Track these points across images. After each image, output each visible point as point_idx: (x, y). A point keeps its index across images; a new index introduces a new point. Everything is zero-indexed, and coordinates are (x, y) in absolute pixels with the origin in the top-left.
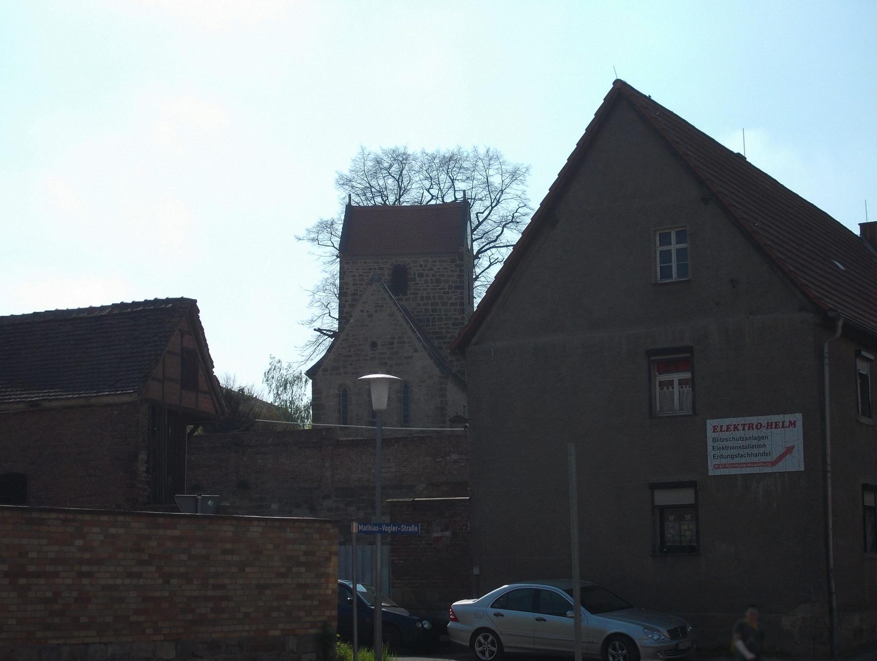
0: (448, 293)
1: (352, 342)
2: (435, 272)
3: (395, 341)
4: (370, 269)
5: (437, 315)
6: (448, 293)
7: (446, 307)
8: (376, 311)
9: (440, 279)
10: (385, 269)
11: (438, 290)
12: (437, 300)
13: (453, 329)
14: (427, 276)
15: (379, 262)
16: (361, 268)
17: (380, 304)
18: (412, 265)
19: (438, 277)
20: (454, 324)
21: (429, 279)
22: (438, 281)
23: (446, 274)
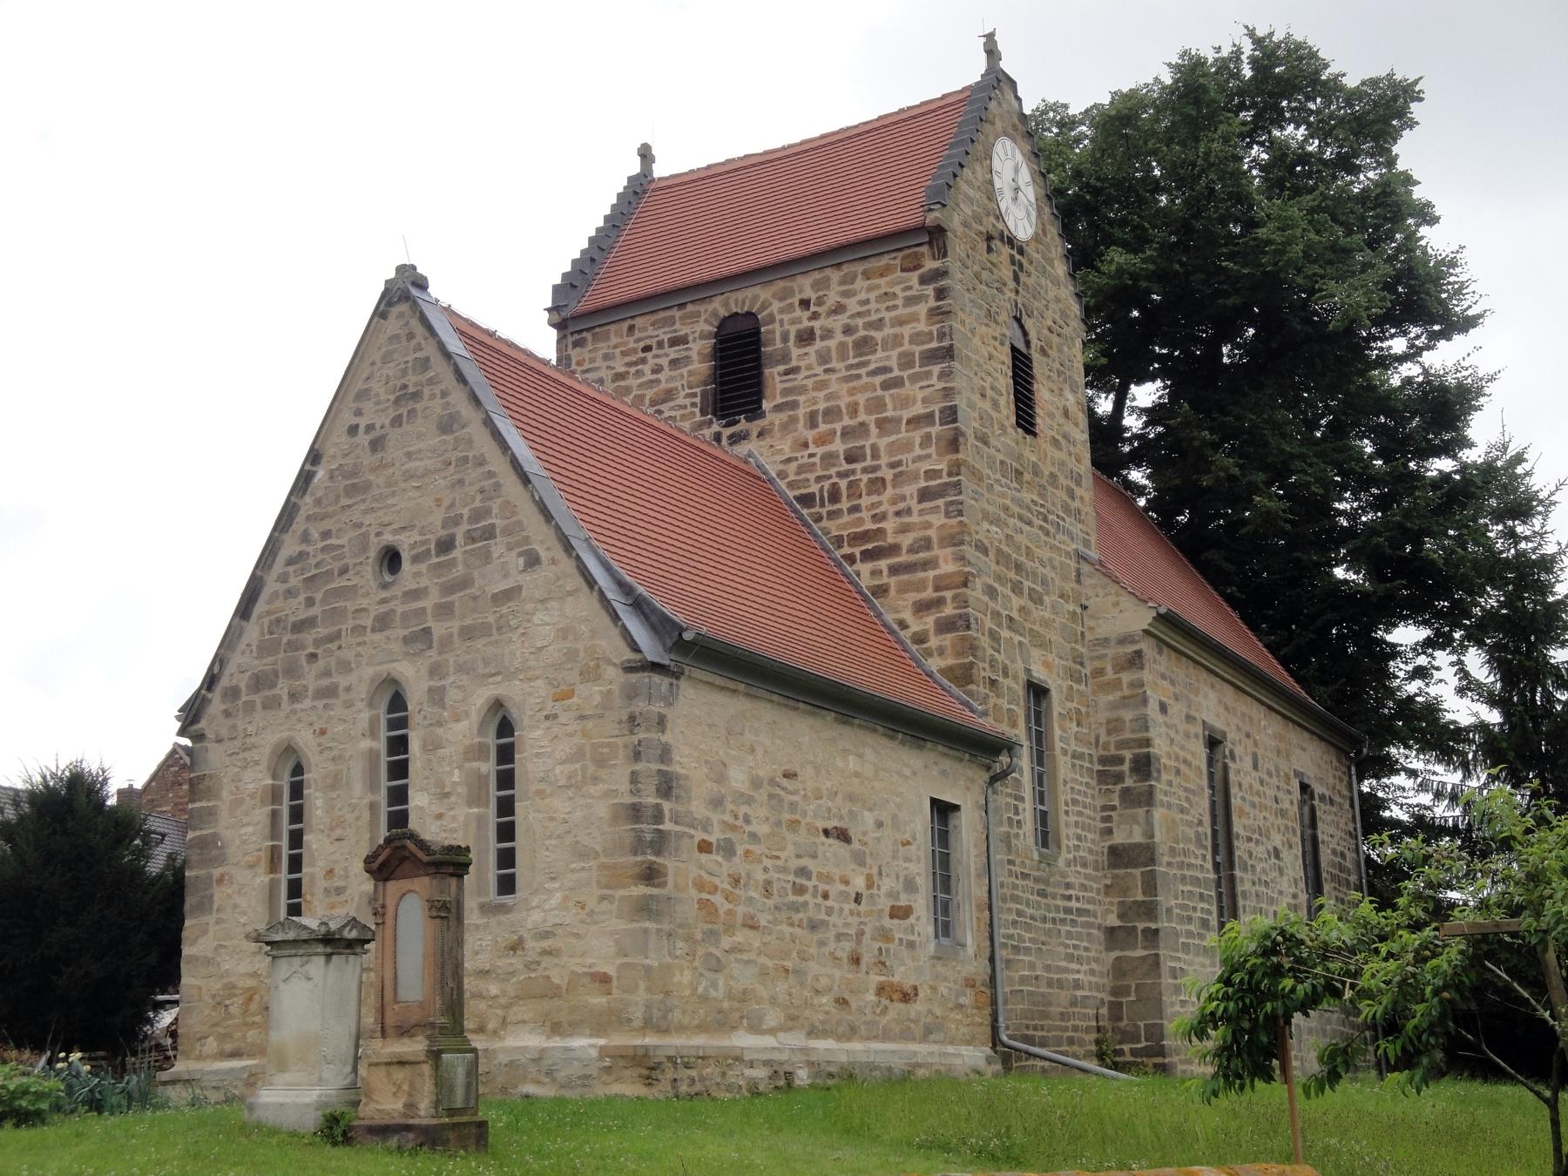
0: (897, 383)
1: (317, 565)
2: (852, 316)
3: (460, 533)
4: (647, 349)
5: (865, 470)
6: (897, 383)
7: (893, 438)
8: (397, 422)
9: (872, 338)
10: (691, 338)
11: (865, 379)
12: (862, 417)
13: (921, 513)
14: (828, 334)
15: (673, 317)
16: (618, 351)
17: (411, 390)
18: (776, 306)
19: (862, 333)
20: (924, 495)
21: (832, 344)
22: (864, 346)
23: (887, 315)
